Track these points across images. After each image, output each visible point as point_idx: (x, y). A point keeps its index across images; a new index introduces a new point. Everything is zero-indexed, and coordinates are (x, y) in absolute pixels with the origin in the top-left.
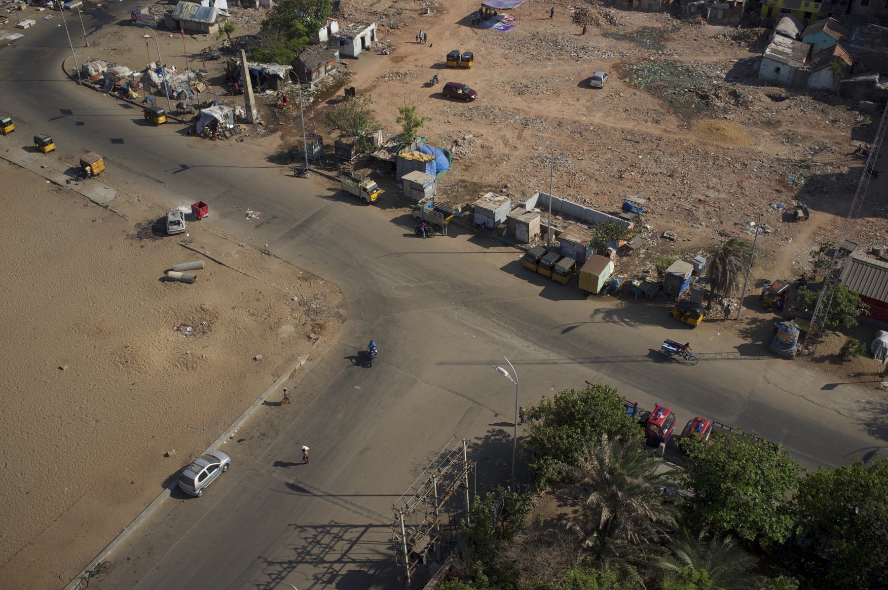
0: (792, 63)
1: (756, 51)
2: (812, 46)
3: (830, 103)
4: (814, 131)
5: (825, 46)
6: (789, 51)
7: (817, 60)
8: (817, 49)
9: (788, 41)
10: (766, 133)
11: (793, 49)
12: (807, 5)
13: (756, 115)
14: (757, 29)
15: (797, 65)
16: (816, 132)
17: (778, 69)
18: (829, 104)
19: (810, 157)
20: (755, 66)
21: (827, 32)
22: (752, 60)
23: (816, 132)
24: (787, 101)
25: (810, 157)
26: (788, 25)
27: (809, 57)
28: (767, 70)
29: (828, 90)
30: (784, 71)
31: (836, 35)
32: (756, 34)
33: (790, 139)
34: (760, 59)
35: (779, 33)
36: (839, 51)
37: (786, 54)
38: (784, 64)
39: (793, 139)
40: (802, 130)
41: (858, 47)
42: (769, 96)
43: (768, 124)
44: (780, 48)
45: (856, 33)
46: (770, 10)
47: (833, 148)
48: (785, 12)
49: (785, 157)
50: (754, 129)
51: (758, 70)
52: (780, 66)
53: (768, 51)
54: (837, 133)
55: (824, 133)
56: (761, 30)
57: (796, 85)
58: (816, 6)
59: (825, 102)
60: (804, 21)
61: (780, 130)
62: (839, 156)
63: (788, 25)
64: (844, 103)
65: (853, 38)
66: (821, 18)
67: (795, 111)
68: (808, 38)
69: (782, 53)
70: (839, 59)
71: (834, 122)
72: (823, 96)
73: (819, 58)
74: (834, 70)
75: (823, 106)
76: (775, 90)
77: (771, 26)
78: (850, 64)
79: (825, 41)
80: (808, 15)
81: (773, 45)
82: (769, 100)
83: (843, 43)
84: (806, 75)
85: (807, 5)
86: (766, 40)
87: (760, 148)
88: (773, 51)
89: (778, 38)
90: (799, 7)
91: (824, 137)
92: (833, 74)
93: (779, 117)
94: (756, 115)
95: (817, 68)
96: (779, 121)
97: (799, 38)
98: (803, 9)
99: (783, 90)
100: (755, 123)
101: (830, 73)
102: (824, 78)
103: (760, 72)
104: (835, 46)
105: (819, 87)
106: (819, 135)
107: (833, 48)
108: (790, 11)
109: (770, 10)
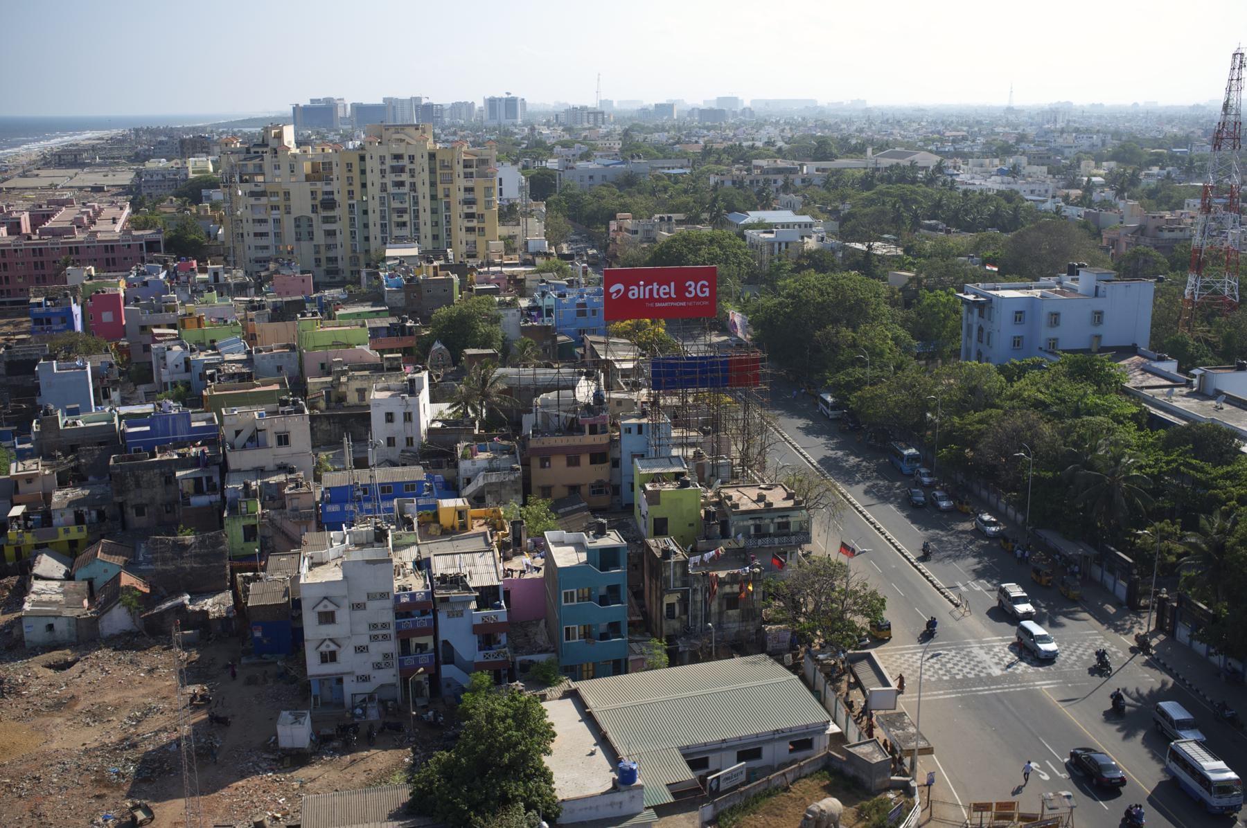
0: (67, 613)
1: (13, 611)
2: (91, 582)
3: (139, 648)
4: (127, 694)
5: (109, 577)
6: (59, 597)
7: (101, 598)
8: (98, 583)
9: (55, 585)
10: (59, 720)
11: (64, 593)
12: (67, 531)
13: (37, 700)
14: (5, 581)
15: (76, 612)
16: (130, 694)
17: (50, 627)
18: (138, 650)
19: (132, 730)
20: (15, 632)
21: (106, 560)
22: (10, 625)
23: (130, 694)
24: (78, 664)
25: (132, 730)
26: (47, 565)
27: (92, 597)
28: (35, 633)
29: (130, 633)
30: (60, 626)
31: (118, 560)
32: (6, 587)
33: (97, 715)
34: (20, 618)
35: (38, 577)
36: (127, 579)
37: (56, 602)
38: (56, 617)
39: (101, 714)
40: (111, 697)
41: (150, 567)
42: (50, 667)
43: (59, 706)
44: (45, 598)
45: (143, 551)
46: (18, 550)
47: (161, 706)
48: (40, 548)
49: (96, 744)
50: (39, 721)
51: (22, 636)
52: (51, 621)
53: (27, 607)
54: (160, 684)
55: (142, 691)
56: (13, 580)
57: (85, 638)
58: (80, 530)
59: (131, 649)
60: (70, 553)
61: (79, 708)
62: (171, 715)
63: (47, 565)
64: (158, 643)
65: (141, 558)
66: (92, 543)
67: (94, 674)
68: (81, 573)
69: (50, 603)
70: (129, 589)
71: (151, 671)
72: (126, 642)
73: (104, 594)
74: (128, 605)
75: (130, 655)
76: (56, 656)
77: (24, 570)
78: (148, 591)
79: (106, 571)
80: (73, 543)
81: (33, 597)
82: (51, 672)
83: (130, 567)
84: (93, 622)
85: (67, 531)
86: (22, 590)
87: (54, 746)
88: (35, 603)
89: (37, 585)
90: (56, 535)
91: (144, 696)
92: (129, 610)
93: (72, 690)
94: (37, 700)
95: (104, 608)
96: (73, 697)
97: (69, 577)
98: (63, 537)
99: (68, 651)
100: (38, 713)
101: (124, 610)
102: (118, 619)
103: (26, 637)
104: (119, 573)
105: (116, 632)
106: (137, 696)
107: (117, 578)
108: (46, 545)
109: (18, 550)
